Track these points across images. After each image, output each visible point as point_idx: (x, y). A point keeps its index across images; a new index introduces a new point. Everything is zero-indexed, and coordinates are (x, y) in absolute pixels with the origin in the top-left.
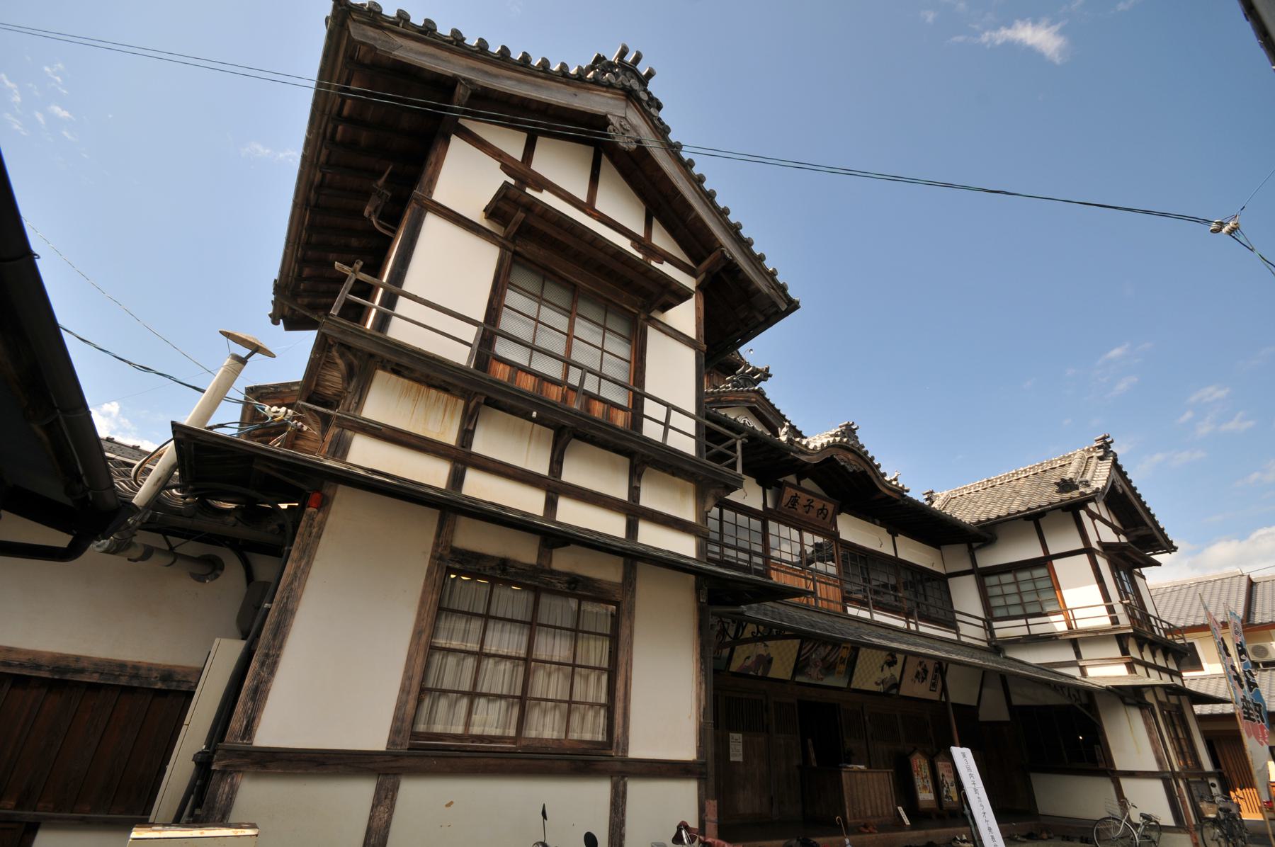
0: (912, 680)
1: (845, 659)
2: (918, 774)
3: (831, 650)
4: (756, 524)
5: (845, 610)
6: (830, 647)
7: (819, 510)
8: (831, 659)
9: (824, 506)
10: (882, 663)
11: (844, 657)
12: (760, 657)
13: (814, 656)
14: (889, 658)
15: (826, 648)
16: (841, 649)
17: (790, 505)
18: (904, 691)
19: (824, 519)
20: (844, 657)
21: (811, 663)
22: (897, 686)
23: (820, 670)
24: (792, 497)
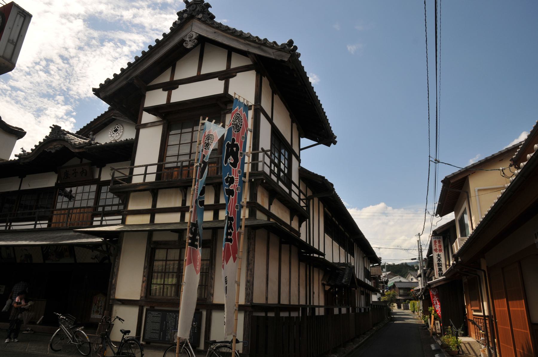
2: (96, 305)
9: (83, 168)
13: (50, 251)
19: (86, 175)
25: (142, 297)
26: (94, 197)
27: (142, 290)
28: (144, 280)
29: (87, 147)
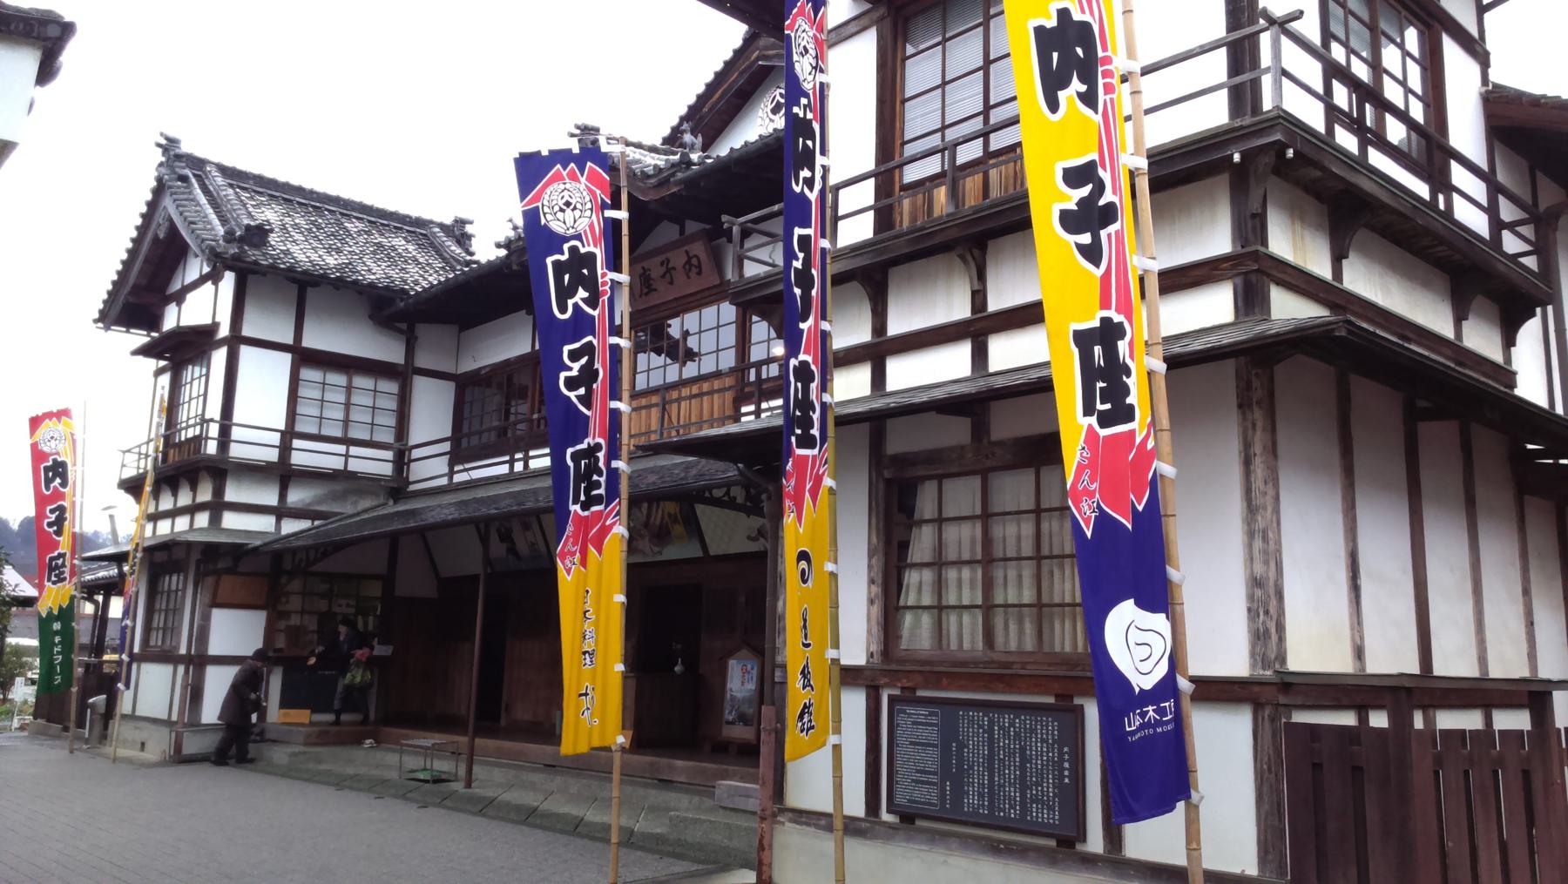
1: (676, 513)
3: (649, 508)
6: (645, 505)
7: (684, 267)
9: (687, 252)
15: (640, 509)
17: (645, 290)
19: (699, 273)
20: (673, 512)
25: (872, 655)
26: (733, 342)
27: (869, 631)
28: (873, 595)
29: (680, 175)
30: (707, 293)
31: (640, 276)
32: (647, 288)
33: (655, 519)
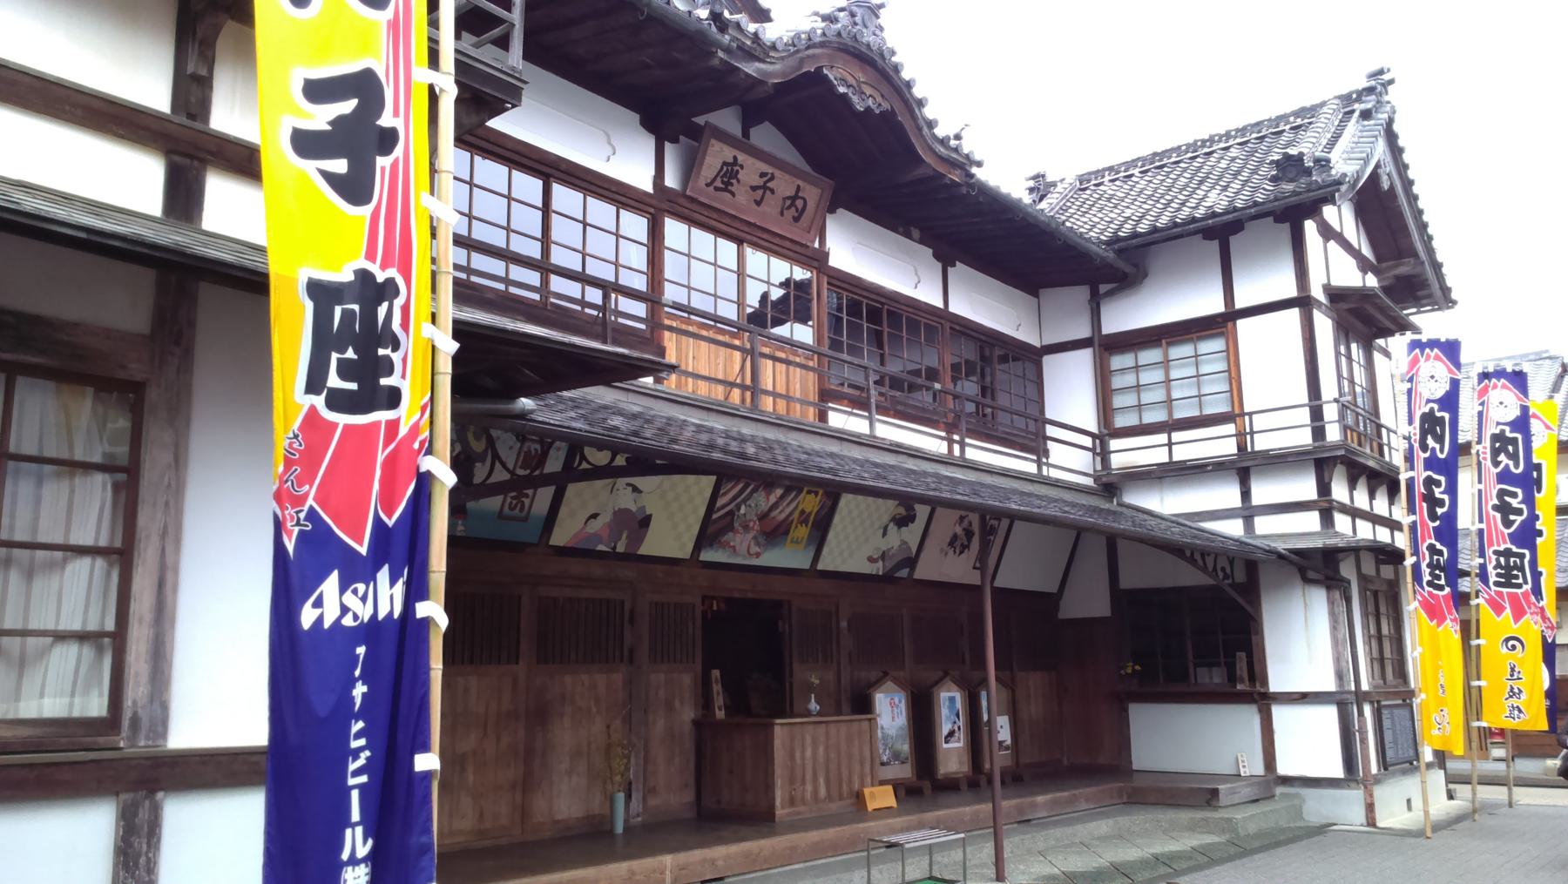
0: (942, 550)
1: (810, 514)
3: (782, 497)
4: (636, 225)
5: (823, 417)
6: (779, 492)
7: (784, 199)
8: (779, 515)
10: (885, 519)
11: (808, 511)
12: (622, 516)
13: (743, 510)
14: (902, 511)
16: (802, 496)
18: (921, 573)
19: (796, 219)
20: (808, 511)
21: (736, 525)
22: (911, 562)
23: (755, 538)
24: (725, 164)
30: (787, 244)
31: (725, 164)
32: (723, 182)
33: (780, 512)
